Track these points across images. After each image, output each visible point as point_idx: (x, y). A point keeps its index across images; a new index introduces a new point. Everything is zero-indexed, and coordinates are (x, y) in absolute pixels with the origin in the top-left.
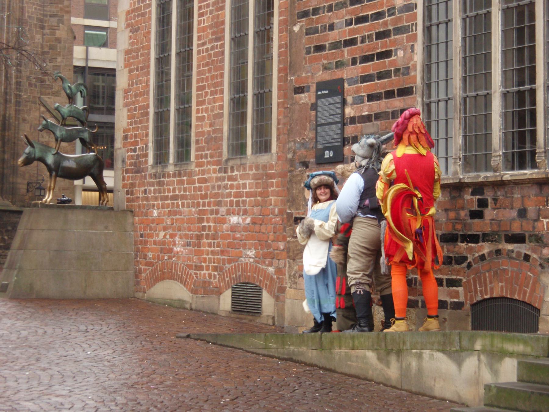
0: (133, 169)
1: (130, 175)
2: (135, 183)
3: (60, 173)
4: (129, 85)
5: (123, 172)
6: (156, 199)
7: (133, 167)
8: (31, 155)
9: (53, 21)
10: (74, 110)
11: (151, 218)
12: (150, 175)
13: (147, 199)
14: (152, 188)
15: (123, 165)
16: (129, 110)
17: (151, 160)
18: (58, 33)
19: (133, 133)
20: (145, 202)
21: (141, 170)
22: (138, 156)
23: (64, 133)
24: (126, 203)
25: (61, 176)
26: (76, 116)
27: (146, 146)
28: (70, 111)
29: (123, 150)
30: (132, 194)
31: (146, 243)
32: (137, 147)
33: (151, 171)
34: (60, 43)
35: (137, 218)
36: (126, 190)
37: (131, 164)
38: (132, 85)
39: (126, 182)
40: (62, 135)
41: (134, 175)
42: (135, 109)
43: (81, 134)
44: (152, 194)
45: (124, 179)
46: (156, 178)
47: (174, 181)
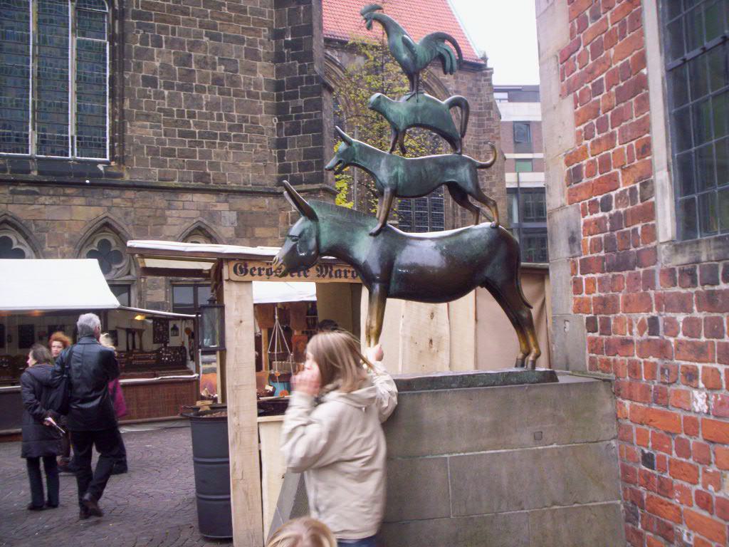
0: (603, 259)
1: (598, 275)
2: (615, 299)
3: (394, 286)
4: (572, 35)
5: (575, 268)
6: (700, 352)
7: (602, 254)
10: (425, 108)
11: (682, 414)
12: (669, 274)
13: (662, 350)
14: (680, 317)
15: (572, 251)
16: (576, 101)
17: (666, 223)
19: (597, 158)
20: (652, 359)
21: (631, 260)
22: (617, 220)
23: (401, 171)
26: (432, 123)
27: (644, 185)
28: (414, 111)
29: (571, 210)
30: (606, 328)
31: (665, 488)
32: (613, 194)
33: (667, 259)
35: (627, 403)
36: (585, 316)
37: (596, 246)
38: (583, 25)
39: (584, 295)
40: (396, 176)
41: (610, 275)
42: (597, 89)
43: (450, 172)
44: (681, 336)
46: (694, 283)
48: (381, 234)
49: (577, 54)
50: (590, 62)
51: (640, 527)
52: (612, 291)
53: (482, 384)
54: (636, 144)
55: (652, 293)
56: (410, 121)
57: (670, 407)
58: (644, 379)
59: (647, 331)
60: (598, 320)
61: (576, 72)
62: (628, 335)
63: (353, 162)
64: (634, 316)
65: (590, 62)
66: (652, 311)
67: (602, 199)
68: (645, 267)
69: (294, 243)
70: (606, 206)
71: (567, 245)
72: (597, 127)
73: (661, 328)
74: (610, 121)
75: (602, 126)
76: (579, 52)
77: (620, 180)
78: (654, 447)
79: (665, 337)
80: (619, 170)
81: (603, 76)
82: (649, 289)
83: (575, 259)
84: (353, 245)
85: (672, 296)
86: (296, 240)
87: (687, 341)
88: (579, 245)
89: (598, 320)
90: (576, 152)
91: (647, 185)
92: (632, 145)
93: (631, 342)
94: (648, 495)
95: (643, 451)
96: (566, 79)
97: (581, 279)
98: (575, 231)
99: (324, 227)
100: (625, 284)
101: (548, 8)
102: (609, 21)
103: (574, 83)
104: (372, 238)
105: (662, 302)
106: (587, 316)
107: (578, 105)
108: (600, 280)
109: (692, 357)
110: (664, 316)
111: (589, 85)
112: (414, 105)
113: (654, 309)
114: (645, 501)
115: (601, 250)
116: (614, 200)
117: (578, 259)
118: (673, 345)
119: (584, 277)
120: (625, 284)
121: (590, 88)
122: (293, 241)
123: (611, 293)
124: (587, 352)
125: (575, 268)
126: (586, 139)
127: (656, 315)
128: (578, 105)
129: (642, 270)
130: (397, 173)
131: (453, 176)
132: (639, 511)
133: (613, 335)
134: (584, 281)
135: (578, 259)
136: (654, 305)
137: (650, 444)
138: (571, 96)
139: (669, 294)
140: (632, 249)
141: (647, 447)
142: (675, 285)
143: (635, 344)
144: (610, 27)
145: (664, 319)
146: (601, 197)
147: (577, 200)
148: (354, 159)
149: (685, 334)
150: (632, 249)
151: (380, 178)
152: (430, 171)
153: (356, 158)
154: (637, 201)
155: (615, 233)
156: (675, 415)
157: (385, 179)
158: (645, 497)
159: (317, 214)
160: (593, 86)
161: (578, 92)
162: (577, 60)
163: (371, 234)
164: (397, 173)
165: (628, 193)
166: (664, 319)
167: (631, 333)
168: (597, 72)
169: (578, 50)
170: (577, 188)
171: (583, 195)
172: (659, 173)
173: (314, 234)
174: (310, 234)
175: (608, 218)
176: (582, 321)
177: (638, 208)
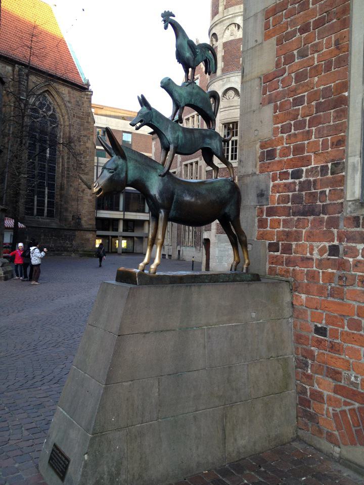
0: (290, 208)
4: (278, 65)
7: (290, 204)
8: (119, 174)
9: (85, 139)
10: (197, 94)
13: (342, 265)
18: (87, 145)
20: (330, 270)
22: (305, 186)
23: (180, 134)
24: (268, 266)
25: (174, 220)
27: (335, 165)
28: (190, 94)
29: (262, 176)
30: (287, 249)
33: (349, 210)
34: (88, 149)
35: (304, 296)
37: (285, 199)
38: (290, 59)
39: (268, 229)
40: (178, 138)
41: (296, 218)
43: (208, 141)
45: (262, 223)
48: (166, 176)
49: (281, 78)
50: (293, 84)
51: (309, 372)
52: (296, 228)
53: (221, 280)
54: (331, 139)
55: (335, 231)
56: (187, 101)
57: (345, 300)
58: (321, 282)
59: (328, 253)
60: (280, 244)
61: (278, 90)
62: (308, 255)
63: (150, 122)
64: (314, 244)
65: (293, 84)
66: (333, 242)
67: (292, 171)
68: (330, 215)
69: (111, 174)
70: (297, 175)
71: (256, 198)
72: (294, 127)
74: (307, 123)
75: (300, 125)
76: (283, 77)
77: (313, 161)
78: (327, 323)
79: (345, 258)
80: (312, 155)
81: (306, 94)
82: (332, 228)
83: (263, 207)
84: (148, 181)
85: (354, 233)
86: (113, 172)
88: (267, 199)
89: (280, 244)
90: (271, 140)
91: (339, 165)
92: (328, 139)
93: (312, 259)
94: (318, 352)
95: (316, 326)
96: (268, 93)
97: (267, 219)
98: (265, 189)
99: (131, 165)
100: (310, 225)
101: (256, 46)
102: (316, 60)
103: (276, 97)
104: (160, 178)
105: (344, 236)
106: (270, 242)
107: (278, 111)
108: (284, 220)
111: (291, 99)
112: (191, 90)
114: (316, 357)
115: (289, 202)
116: (304, 173)
117: (265, 207)
119: (269, 218)
120: (310, 225)
121: (291, 101)
122: (110, 172)
123: (294, 229)
124: (267, 263)
125: (262, 212)
126: (282, 133)
128: (278, 111)
129: (326, 217)
130: (178, 136)
131: (209, 144)
132: (310, 362)
133: (293, 254)
134: (269, 221)
135: (265, 207)
136: (336, 238)
137: (324, 322)
138: (272, 105)
139: (353, 232)
140: (318, 203)
141: (321, 323)
143: (315, 261)
144: (316, 63)
146: (292, 170)
147: (269, 170)
148: (151, 120)
150: (318, 203)
151: (168, 137)
152: (197, 138)
153: (153, 120)
154: (327, 174)
155: (304, 193)
156: (350, 305)
157: (171, 138)
158: (316, 354)
159: (126, 154)
160: (293, 100)
161: (278, 103)
162: (280, 82)
163: (160, 176)
164: (178, 136)
165: (319, 169)
167: (311, 254)
168: (298, 91)
169: (282, 75)
170: (269, 163)
171: (275, 167)
172: (351, 158)
173: (125, 170)
174: (122, 169)
175: (298, 183)
176: (266, 245)
177: (327, 178)
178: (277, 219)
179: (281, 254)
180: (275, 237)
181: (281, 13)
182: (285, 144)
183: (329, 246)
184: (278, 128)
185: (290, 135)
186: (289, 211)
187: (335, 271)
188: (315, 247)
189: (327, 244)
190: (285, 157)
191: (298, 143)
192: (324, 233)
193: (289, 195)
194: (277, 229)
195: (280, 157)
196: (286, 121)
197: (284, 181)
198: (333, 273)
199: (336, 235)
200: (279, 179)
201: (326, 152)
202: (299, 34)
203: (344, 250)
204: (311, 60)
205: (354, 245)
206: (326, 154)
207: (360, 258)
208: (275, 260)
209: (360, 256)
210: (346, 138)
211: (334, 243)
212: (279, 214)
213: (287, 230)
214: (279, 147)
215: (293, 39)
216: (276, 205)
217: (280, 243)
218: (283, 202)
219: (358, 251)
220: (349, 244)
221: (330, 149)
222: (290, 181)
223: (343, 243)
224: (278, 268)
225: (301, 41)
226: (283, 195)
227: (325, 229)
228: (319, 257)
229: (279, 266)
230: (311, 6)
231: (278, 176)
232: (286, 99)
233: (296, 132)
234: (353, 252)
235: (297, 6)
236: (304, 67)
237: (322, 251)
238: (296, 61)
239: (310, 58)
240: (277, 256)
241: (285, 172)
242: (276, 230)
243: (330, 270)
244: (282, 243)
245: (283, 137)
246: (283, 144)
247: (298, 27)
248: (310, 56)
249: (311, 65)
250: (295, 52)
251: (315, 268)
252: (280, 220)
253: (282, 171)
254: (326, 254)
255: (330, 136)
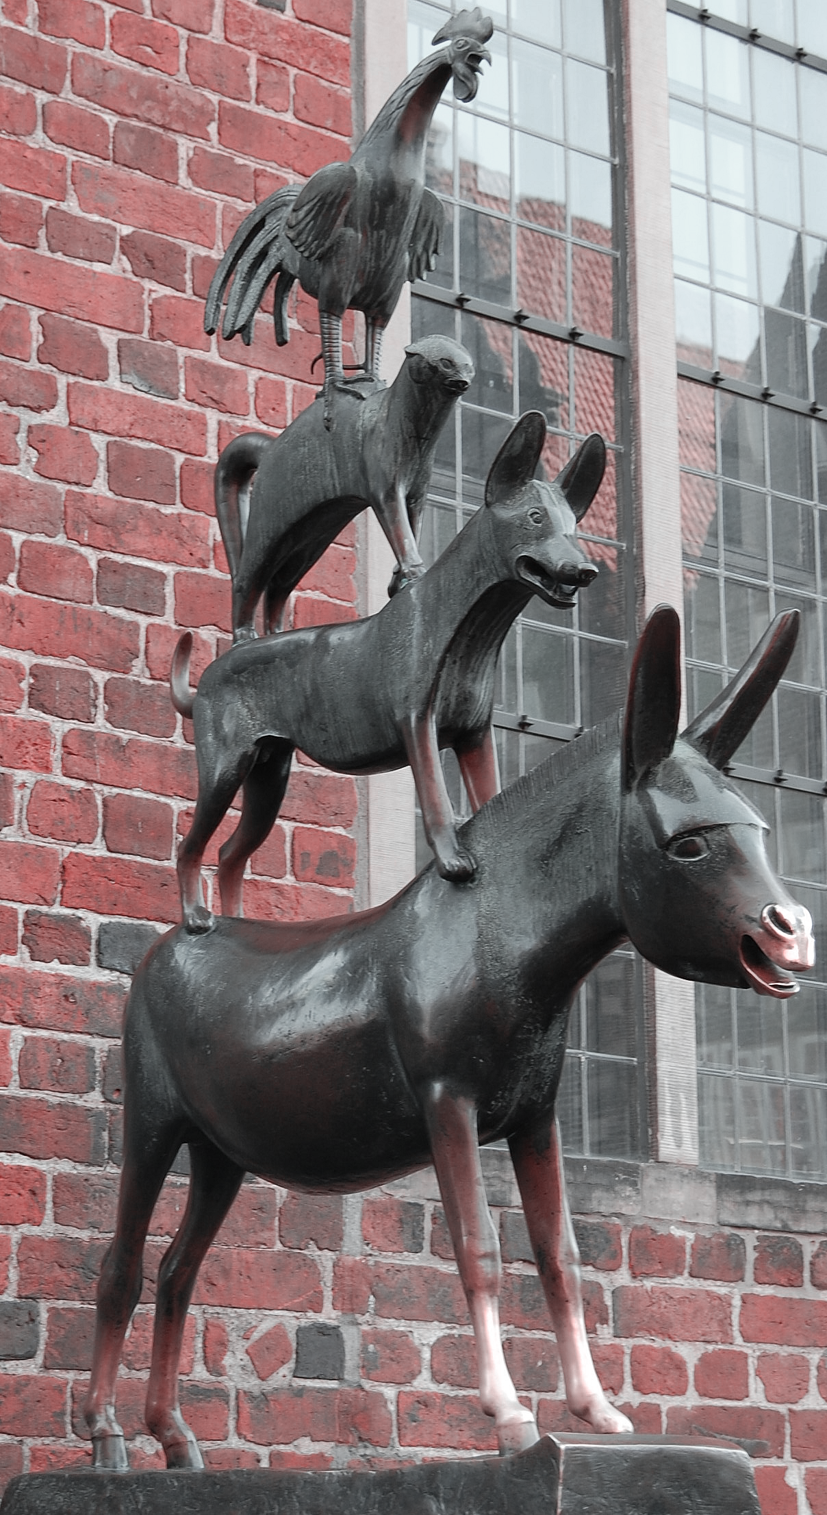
13: (355, 1420)
20: (306, 1447)
37: (65, 1069)
47: (725, 1302)
49: (29, 418)
55: (326, 1259)
60: (44, 1316)
61: (13, 470)
62: (200, 1373)
65: (100, 487)
67: (103, 929)
73: (351, 1359)
76: (36, 419)
79: (367, 1385)
81: (168, 569)
85: (406, 1275)
87: (445, 1397)
89: (44, 1316)
93: (222, 1394)
105: (365, 1288)
107: (12, 578)
108: (61, 1182)
109: (466, 1436)
110: (365, 1328)
113: (327, 1305)
115: (93, 1089)
118: (392, 1408)
121: (93, 565)
127: (334, 1323)
136: (328, 1294)
142: (417, 1249)
145: (365, 1335)
146: (104, 919)
149: (436, 1378)
166: (365, 1335)
167: (214, 1367)
169: (37, 410)
178: (20, 1168)
179: (46, 1367)
180: (13, 1275)
181: (21, 89)
182: (57, 767)
183: (299, 1330)
184: (16, 669)
185: (91, 735)
186: (99, 1136)
187: (325, 1448)
188: (233, 1337)
189: (291, 1321)
190: (65, 838)
191: (136, 793)
192: (279, 1267)
193: (92, 1050)
194: (26, 1229)
195: (35, 830)
196: (62, 656)
197: (55, 965)
198: (321, 1455)
199: (328, 1276)
200: (24, 948)
201: (274, 886)
202: (128, 266)
203: (364, 1349)
204: (189, 426)
205: (401, 1326)
206: (273, 897)
207: (423, 1383)
208: (11, 1407)
209: (426, 1374)
210: (359, 855)
211: (321, 1318)
212: (32, 1140)
213: (85, 1235)
214: (20, 776)
215: (98, 267)
216: (13, 1090)
217: (43, 1307)
218: (59, 1081)
219: (418, 1353)
220: (386, 1325)
221: (289, 880)
222: (92, 973)
223: (360, 1319)
224: (26, 1451)
225: (141, 306)
226: (58, 1043)
227: (279, 1246)
228: (252, 1384)
229: (29, 1442)
230: (184, 179)
231: (20, 934)
232: (60, 540)
233: (125, 735)
234: (393, 1358)
235: (111, 119)
236: (159, 442)
237: (264, 1355)
238: (114, 382)
239: (189, 417)
240: (28, 1379)
241: (64, 919)
242: (15, 1235)
243: (306, 1447)
244: (54, 1313)
245: (45, 728)
246: (47, 769)
247: (126, 230)
248: (182, 404)
249: (192, 449)
250: (109, 338)
251: (234, 1442)
252: (41, 1176)
253: (44, 909)
254: (286, 1370)
255: (294, 819)
